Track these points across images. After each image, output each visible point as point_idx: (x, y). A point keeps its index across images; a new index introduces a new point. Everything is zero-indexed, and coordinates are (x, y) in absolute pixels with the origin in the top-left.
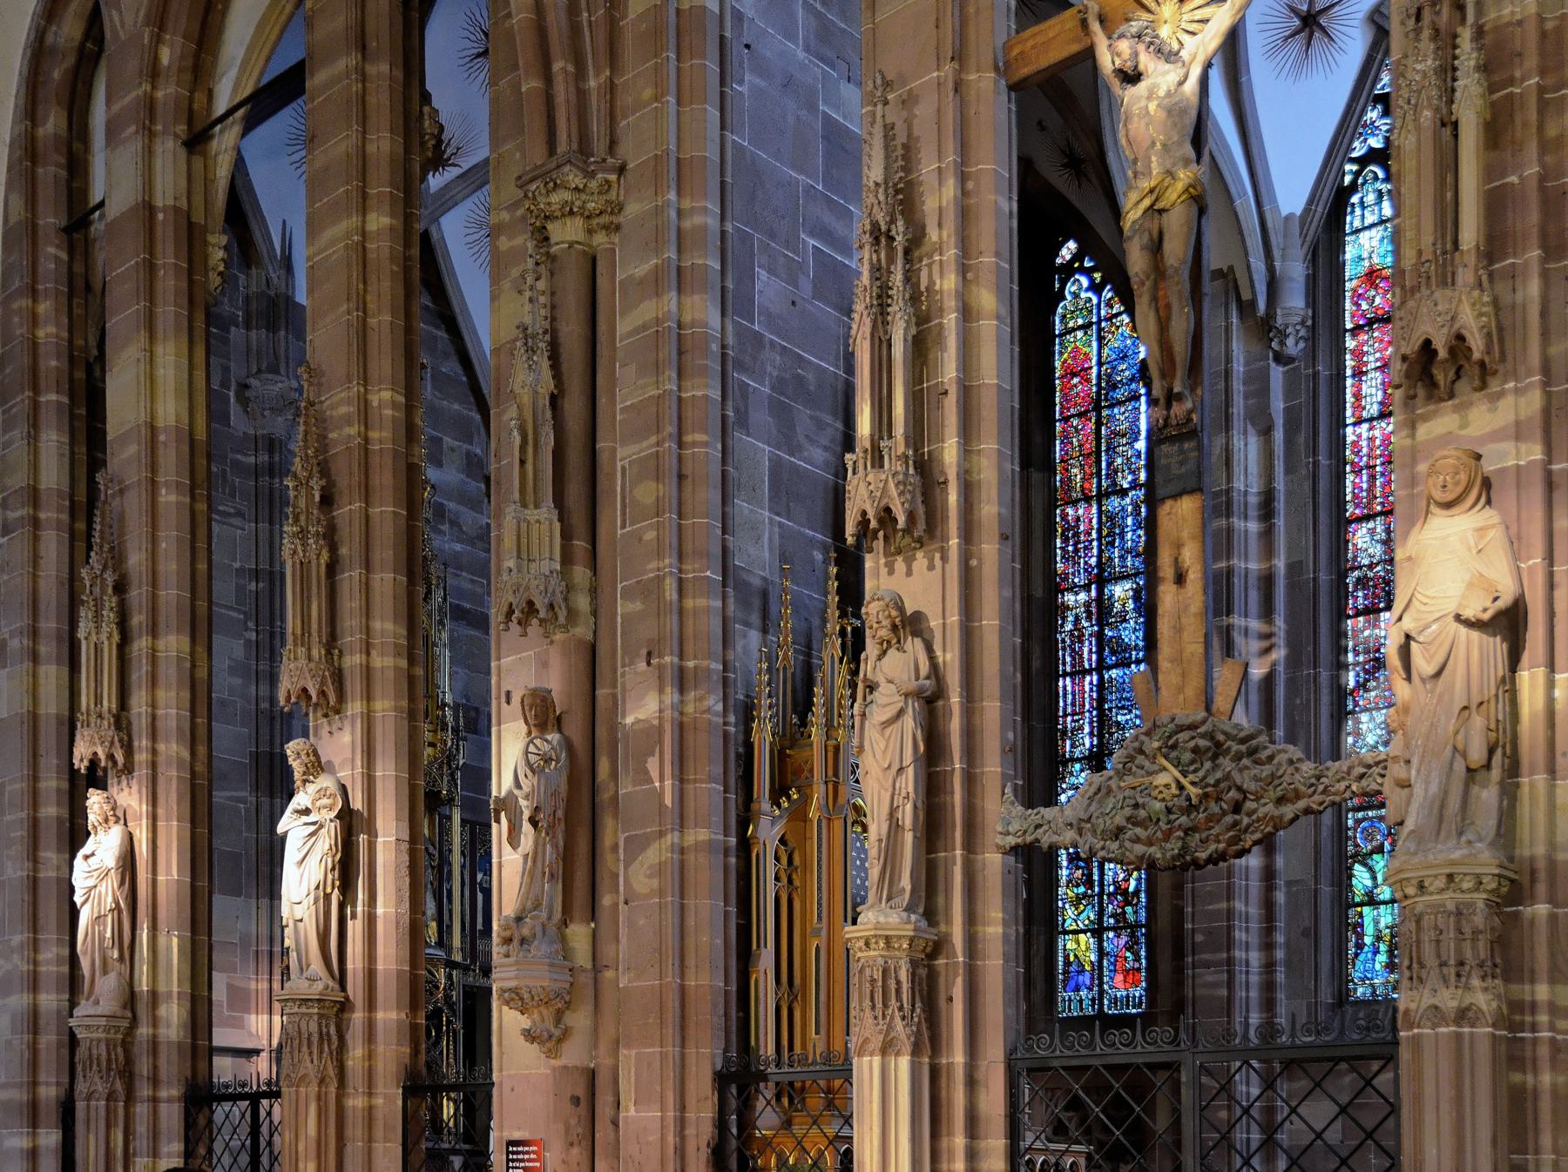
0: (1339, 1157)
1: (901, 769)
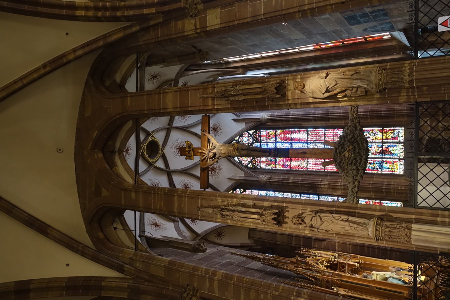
0: (447, 4)
1: (333, 217)
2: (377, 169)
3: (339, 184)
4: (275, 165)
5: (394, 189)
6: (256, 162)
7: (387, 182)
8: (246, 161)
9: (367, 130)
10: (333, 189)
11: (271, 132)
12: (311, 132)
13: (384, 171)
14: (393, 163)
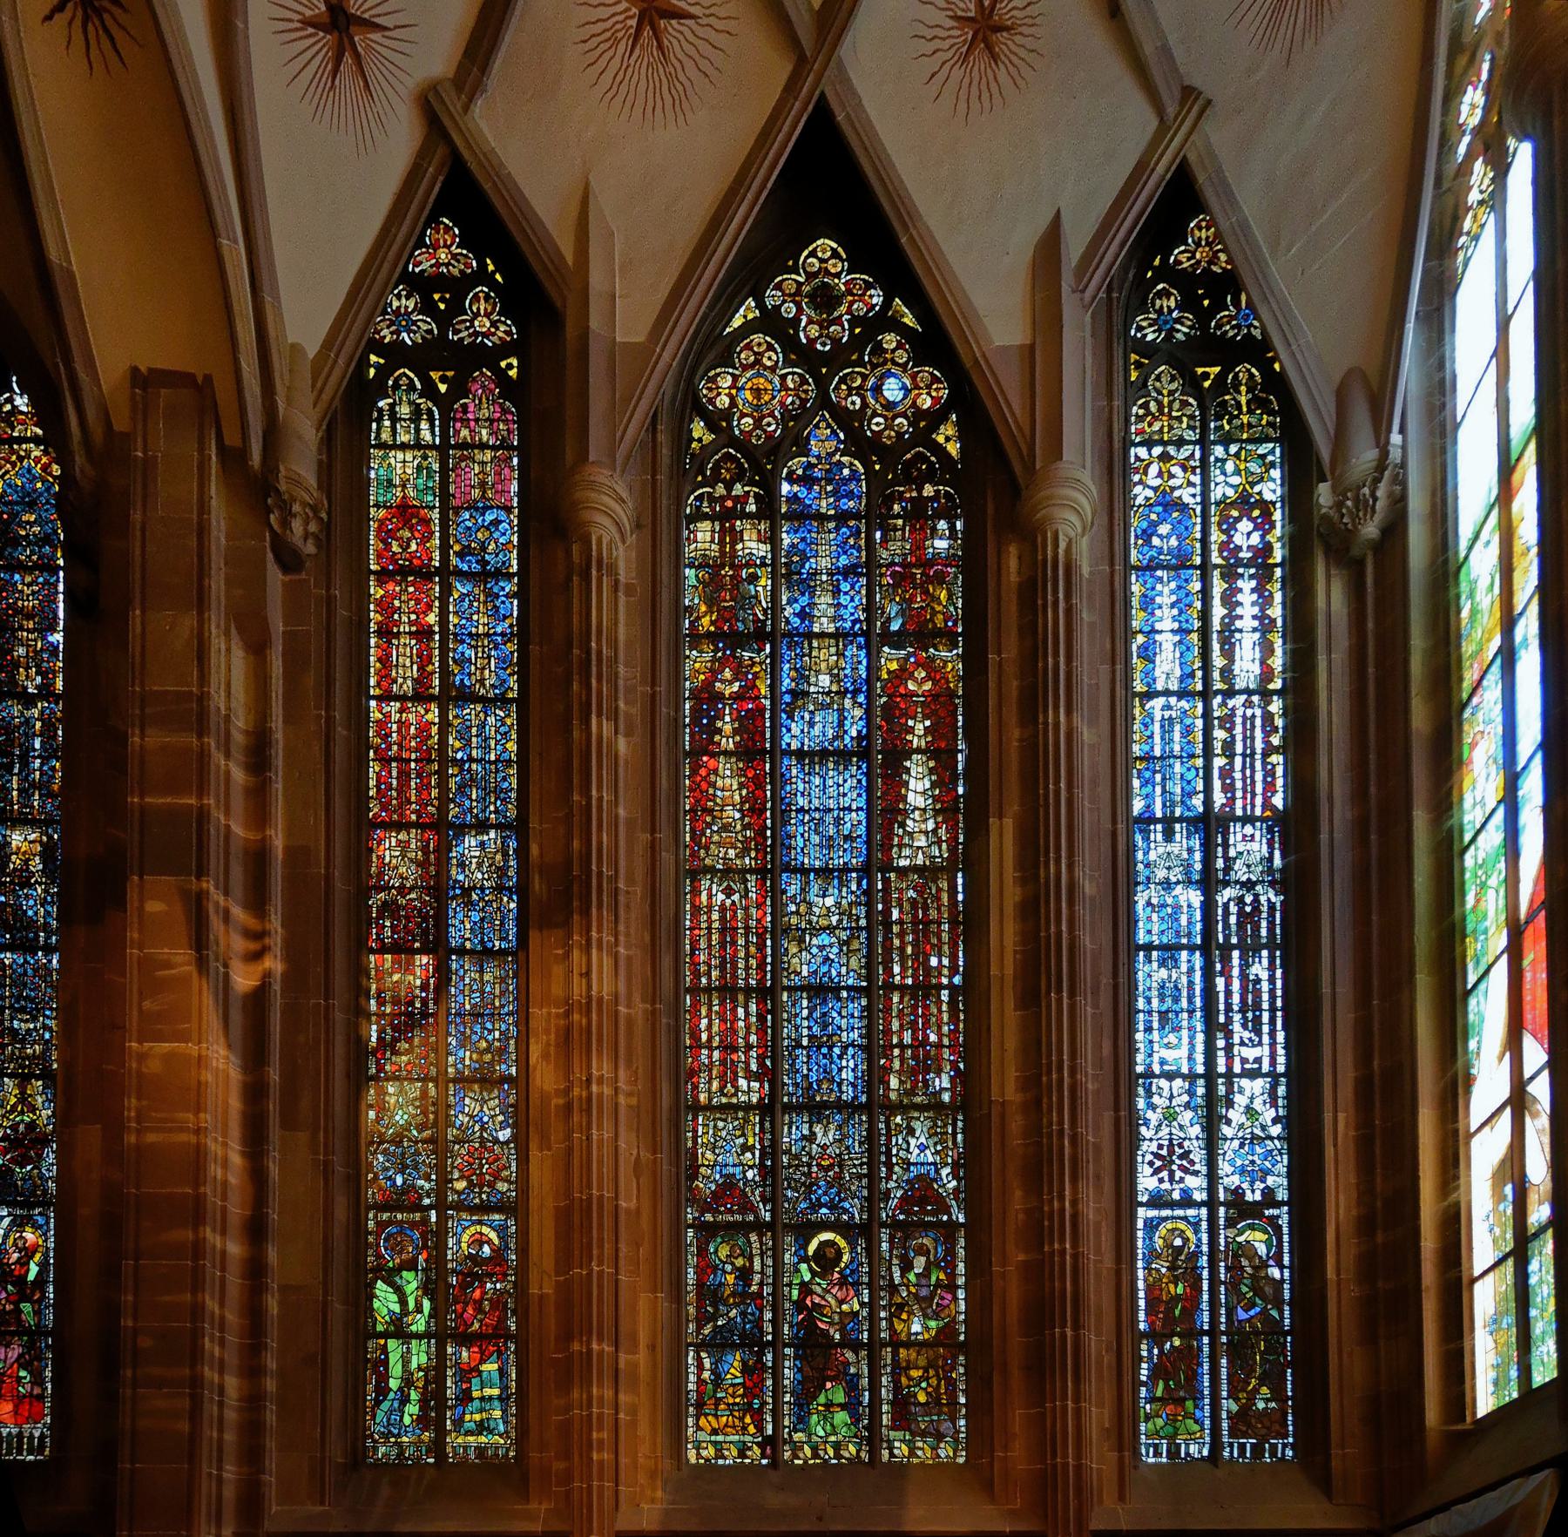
2: (714, 1318)
3: (600, 1068)
4: (708, 635)
5: (590, 1405)
6: (729, 487)
7: (634, 1366)
8: (733, 404)
9: (951, 1252)
10: (566, 1037)
11: (943, 595)
12: (945, 897)
13: (699, 1360)
14: (750, 1404)
